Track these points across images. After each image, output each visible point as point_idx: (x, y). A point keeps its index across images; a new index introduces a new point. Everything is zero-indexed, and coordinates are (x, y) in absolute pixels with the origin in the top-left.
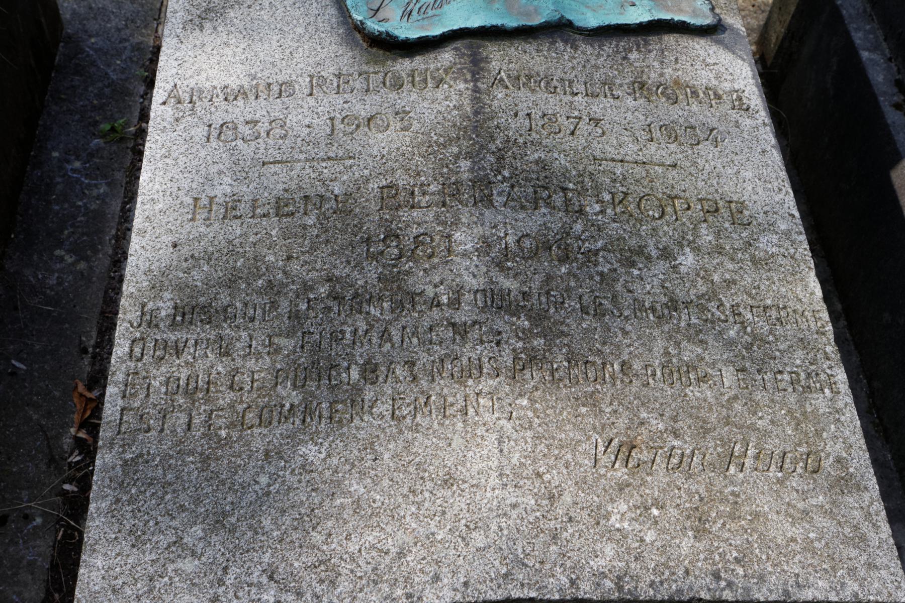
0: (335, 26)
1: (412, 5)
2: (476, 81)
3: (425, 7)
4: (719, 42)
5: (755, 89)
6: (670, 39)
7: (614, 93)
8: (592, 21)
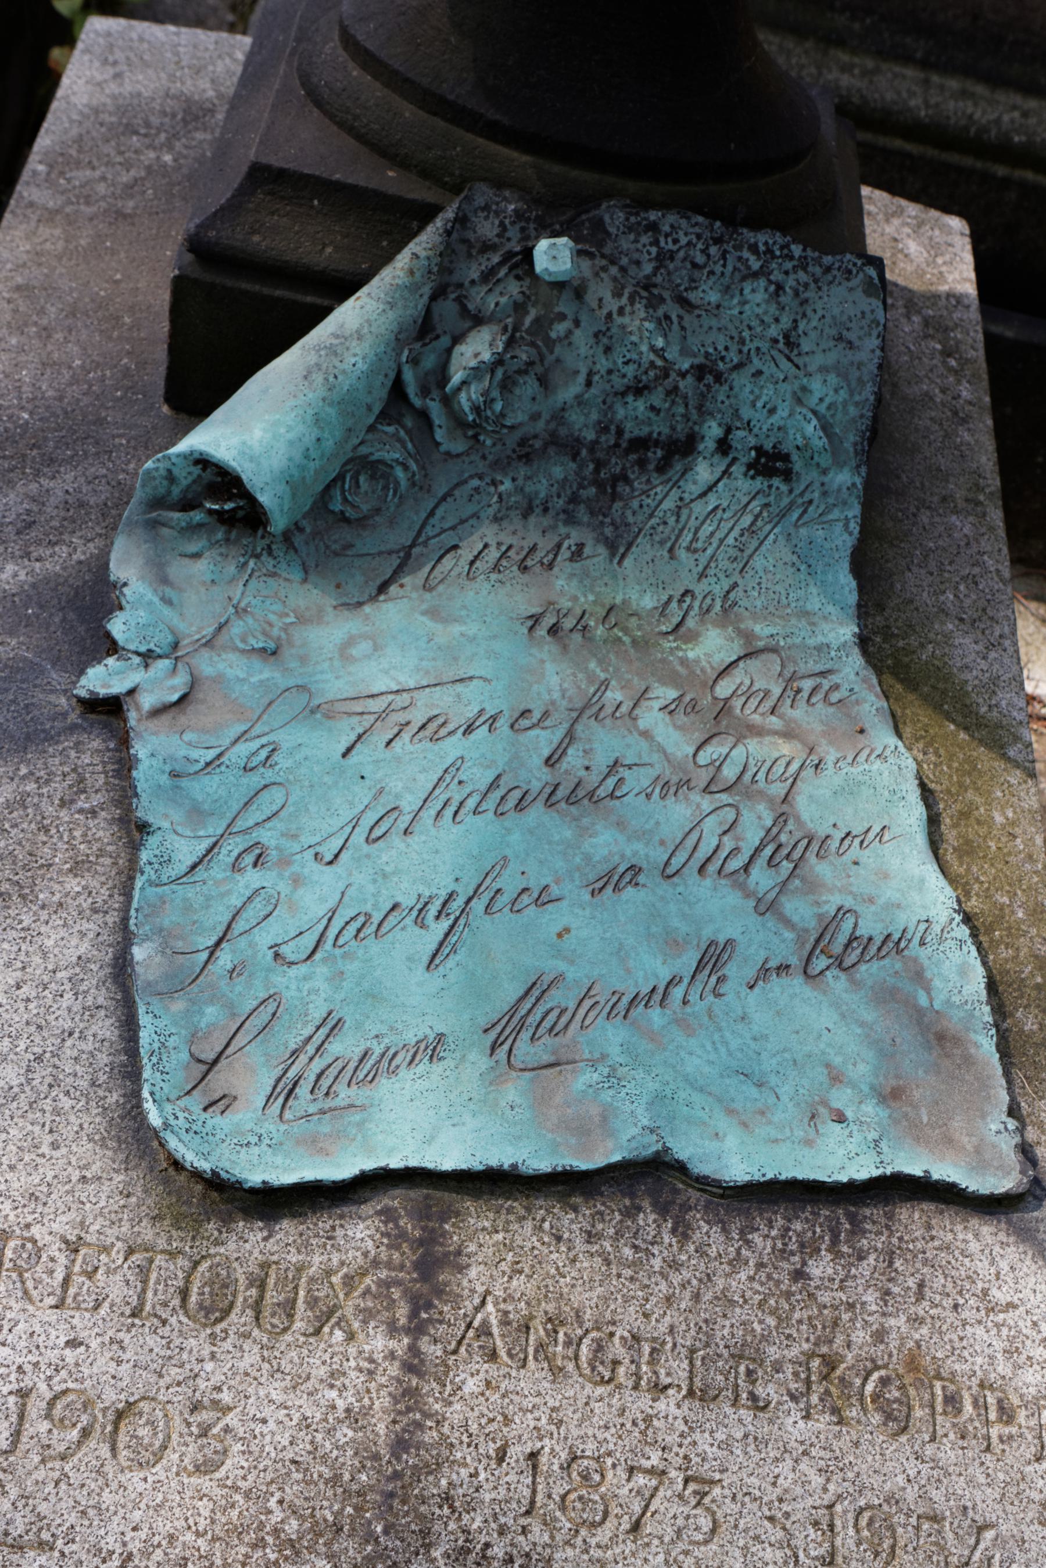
0: (102, 1078)
1: (303, 1059)
2: (417, 1329)
3: (333, 1072)
6: (912, 1217)
7: (760, 1391)
8: (737, 1162)
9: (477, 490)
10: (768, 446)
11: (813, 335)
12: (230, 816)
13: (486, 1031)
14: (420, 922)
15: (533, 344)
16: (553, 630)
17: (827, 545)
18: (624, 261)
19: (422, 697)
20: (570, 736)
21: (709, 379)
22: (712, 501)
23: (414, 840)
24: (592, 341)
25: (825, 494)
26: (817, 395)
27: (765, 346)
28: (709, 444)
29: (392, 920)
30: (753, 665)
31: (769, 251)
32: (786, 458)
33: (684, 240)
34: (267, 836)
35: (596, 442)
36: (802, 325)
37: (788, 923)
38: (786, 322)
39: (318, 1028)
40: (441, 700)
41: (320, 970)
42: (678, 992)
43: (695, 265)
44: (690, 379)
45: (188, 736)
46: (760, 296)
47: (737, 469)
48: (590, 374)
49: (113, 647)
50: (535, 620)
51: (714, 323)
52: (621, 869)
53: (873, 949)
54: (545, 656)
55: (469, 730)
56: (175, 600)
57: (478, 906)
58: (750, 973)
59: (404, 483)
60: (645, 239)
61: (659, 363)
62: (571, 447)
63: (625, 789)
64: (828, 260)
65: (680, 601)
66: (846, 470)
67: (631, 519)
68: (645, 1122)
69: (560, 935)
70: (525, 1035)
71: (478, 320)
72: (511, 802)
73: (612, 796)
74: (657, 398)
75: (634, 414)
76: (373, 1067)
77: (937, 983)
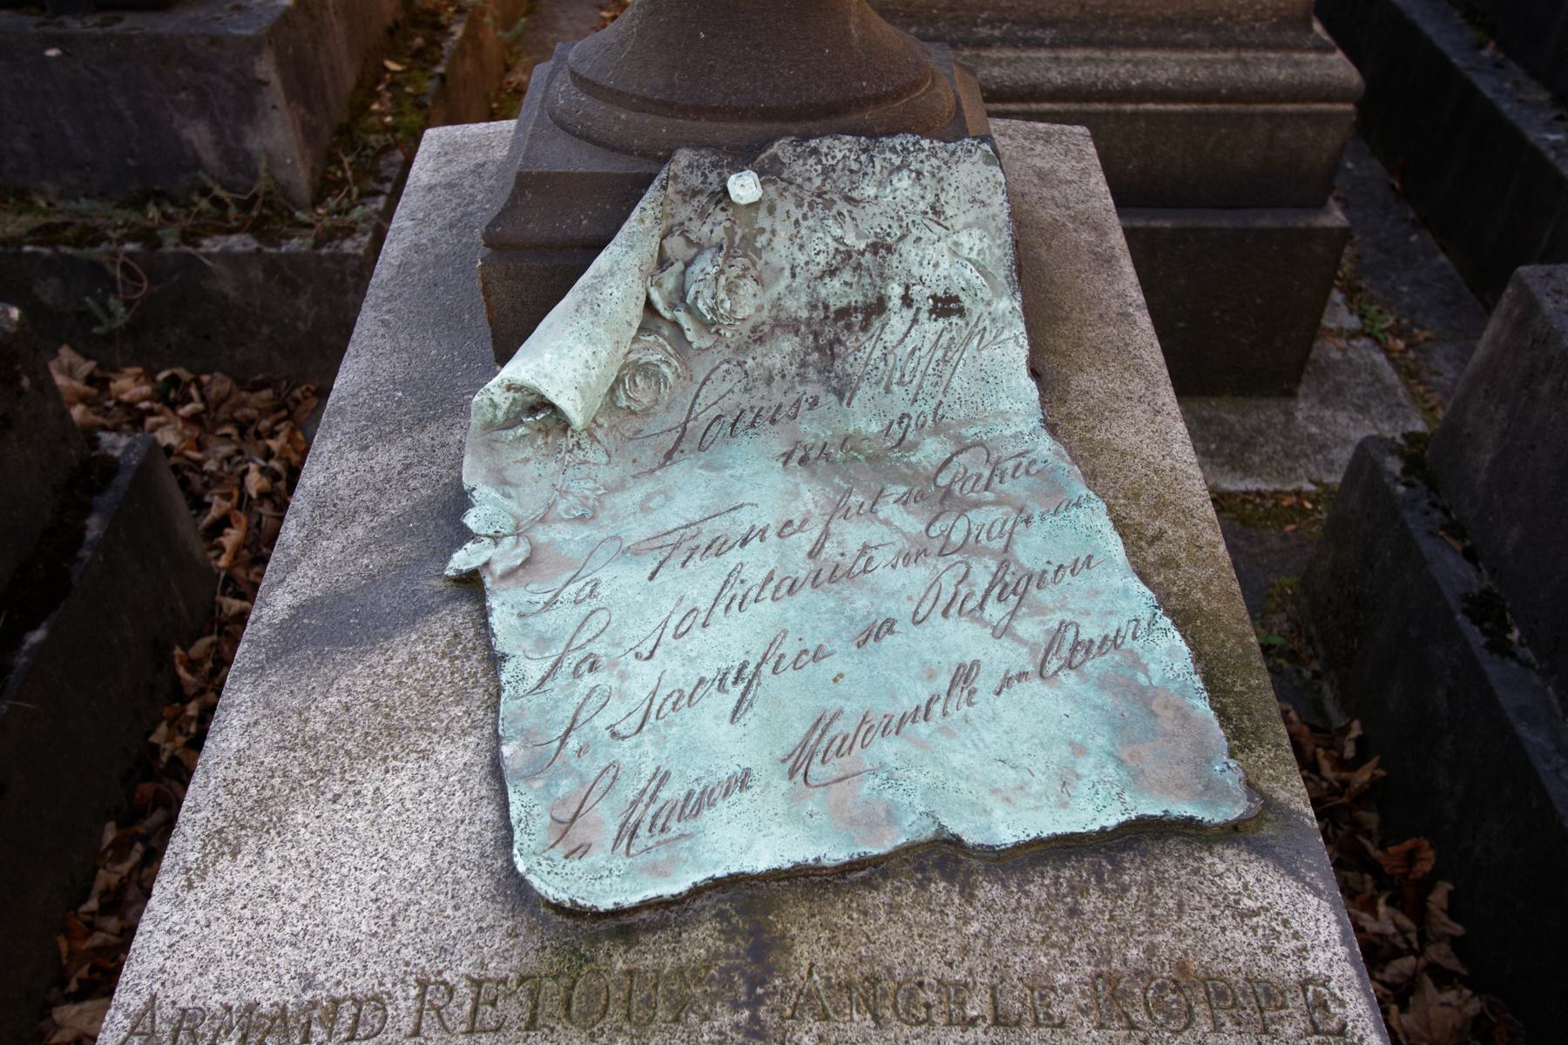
0: (489, 850)
1: (641, 807)
3: (665, 813)
4: (1262, 850)
5: (1351, 972)
7: (1055, 1011)
8: (1008, 829)
9: (727, 371)
10: (940, 294)
11: (953, 202)
12: (568, 637)
13: (784, 761)
14: (721, 688)
15: (745, 255)
16: (802, 461)
17: (1005, 359)
18: (799, 180)
19: (705, 527)
20: (826, 534)
21: (882, 252)
22: (909, 344)
23: (710, 630)
24: (788, 243)
25: (993, 320)
26: (967, 246)
27: (918, 219)
28: (895, 302)
29: (700, 691)
30: (964, 458)
31: (905, 149)
32: (956, 299)
33: (839, 156)
34: (597, 648)
35: (810, 318)
36: (943, 198)
37: (1021, 641)
38: (930, 197)
39: (650, 781)
40: (720, 525)
41: (647, 737)
42: (937, 708)
43: (851, 171)
44: (868, 256)
45: (531, 587)
46: (906, 183)
47: (923, 316)
48: (793, 268)
49: (466, 535)
50: (788, 457)
51: (876, 210)
52: (879, 623)
53: (1095, 649)
54: (799, 480)
55: (745, 542)
56: (513, 493)
57: (766, 669)
58: (995, 683)
59: (671, 378)
60: (811, 161)
61: (842, 248)
62: (793, 326)
63: (874, 565)
64: (951, 146)
65: (900, 423)
66: (1005, 298)
67: (850, 371)
68: (922, 809)
69: (835, 680)
70: (817, 759)
72: (784, 590)
73: (865, 571)
74: (847, 275)
75: (836, 291)
76: (697, 803)
77: (1152, 666)
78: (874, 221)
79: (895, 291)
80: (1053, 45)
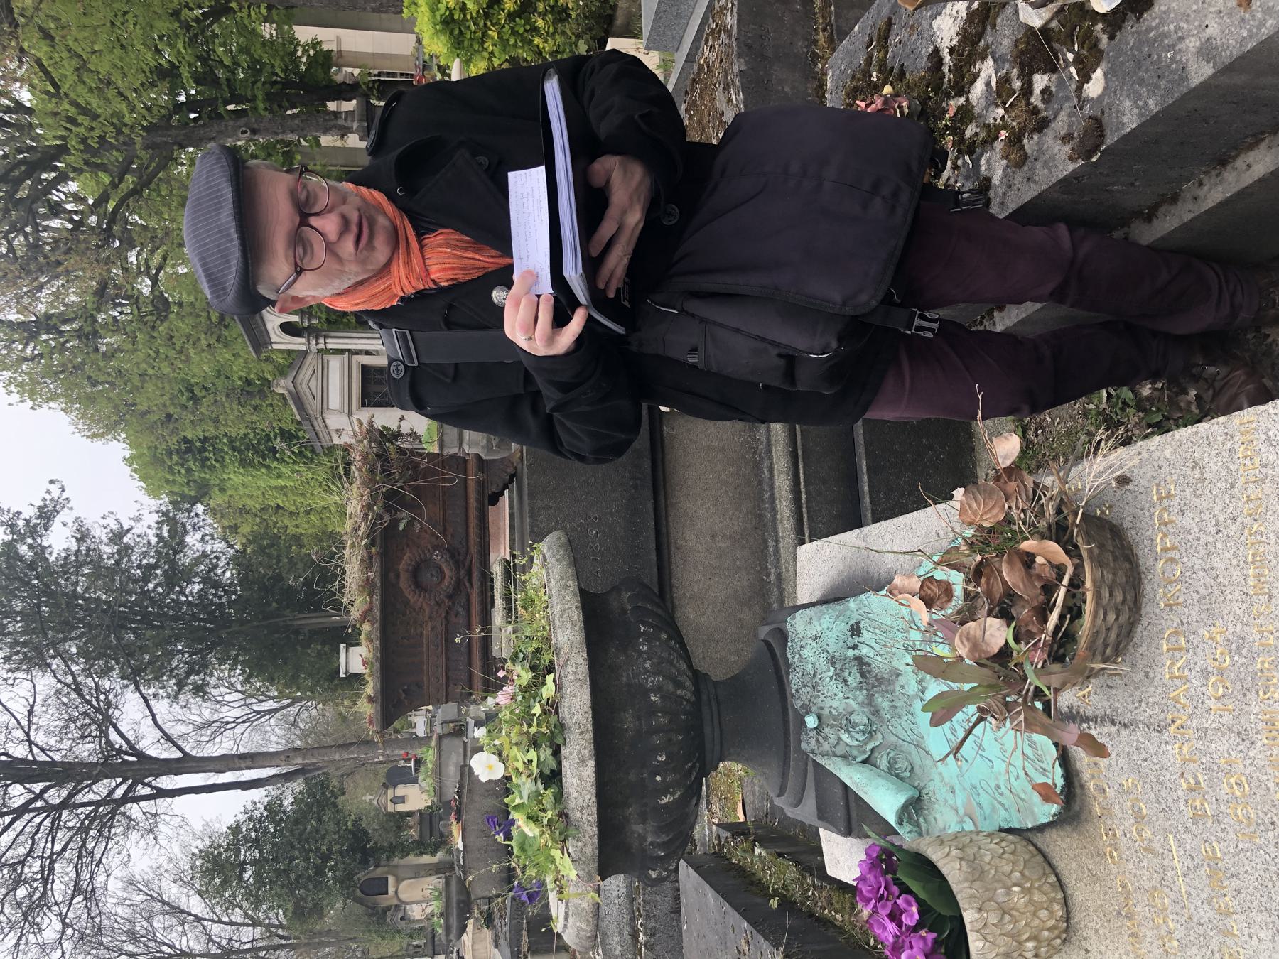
22: (874, 645)
28: (856, 652)
47: (861, 639)
62: (870, 697)
71: (839, 739)
74: (846, 674)
75: (854, 679)
78: (822, 664)
79: (851, 653)
80: (777, 541)
